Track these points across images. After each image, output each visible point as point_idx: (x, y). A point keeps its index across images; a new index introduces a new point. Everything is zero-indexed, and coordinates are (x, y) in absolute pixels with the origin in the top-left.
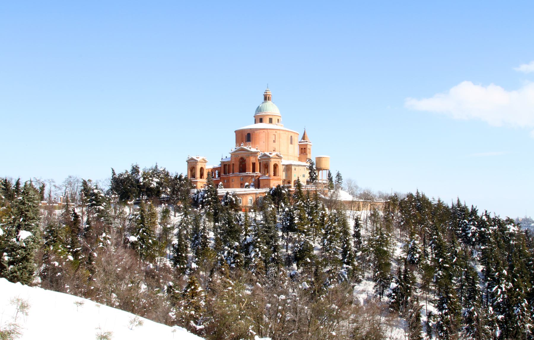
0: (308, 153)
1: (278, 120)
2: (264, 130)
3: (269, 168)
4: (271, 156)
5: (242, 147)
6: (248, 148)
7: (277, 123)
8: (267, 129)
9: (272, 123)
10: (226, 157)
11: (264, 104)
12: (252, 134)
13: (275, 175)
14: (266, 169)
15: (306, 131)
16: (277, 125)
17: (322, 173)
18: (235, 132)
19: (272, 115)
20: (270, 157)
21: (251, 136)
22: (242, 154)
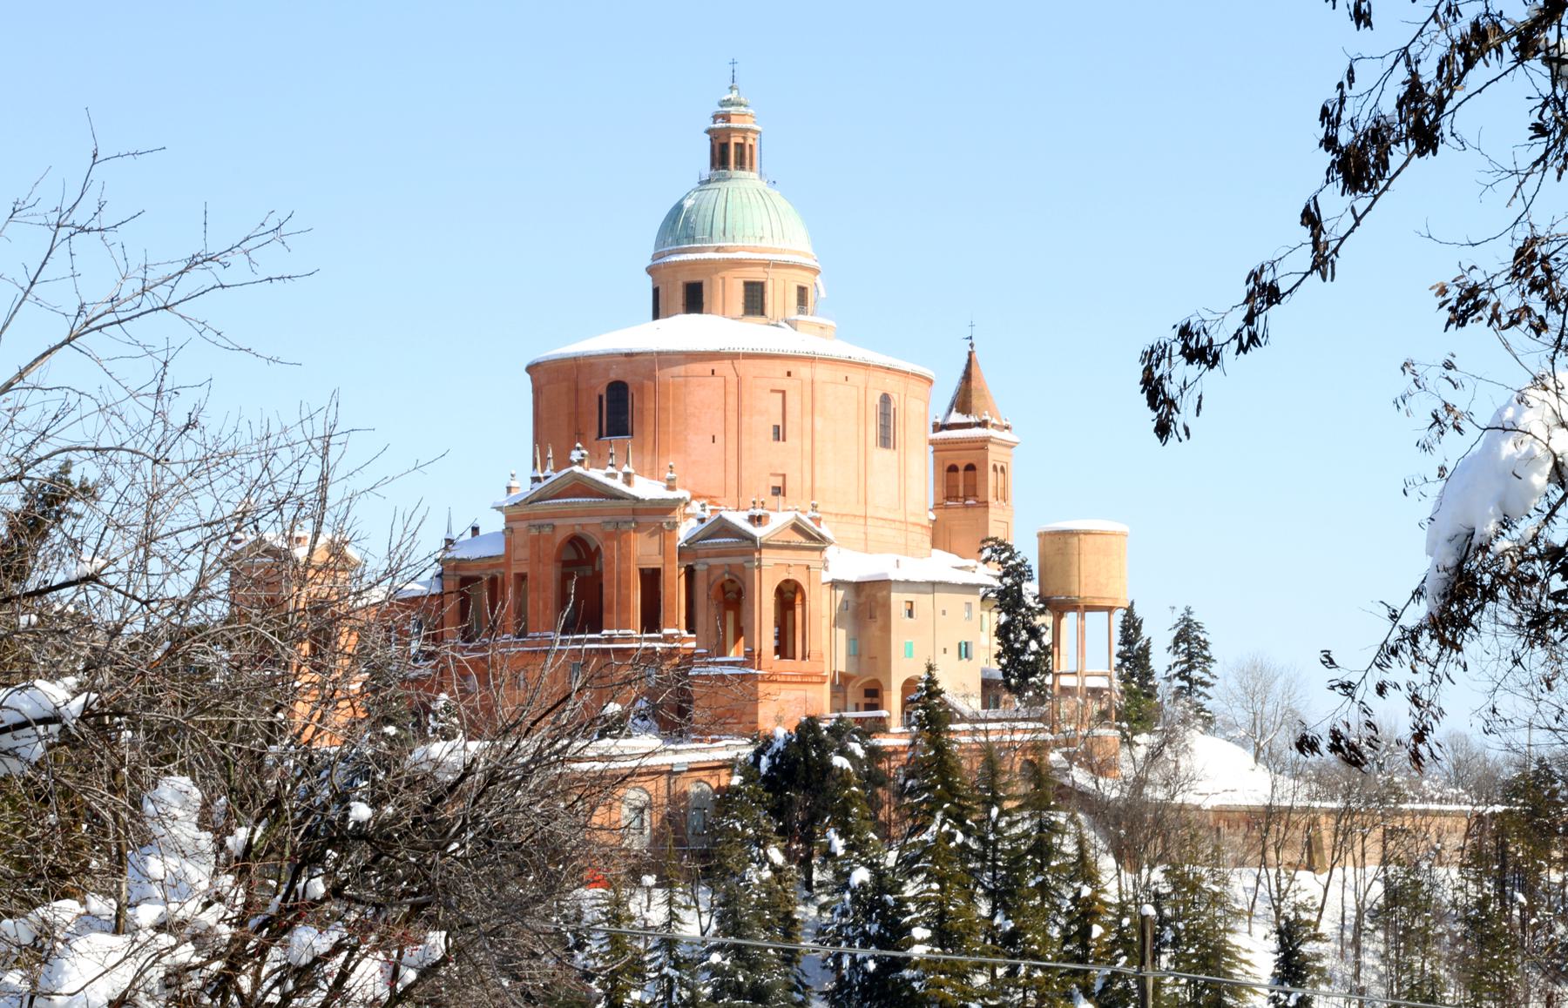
0: (991, 499)
1: (802, 291)
2: (715, 365)
3: (745, 606)
4: (759, 532)
5: (577, 469)
6: (613, 476)
7: (793, 314)
8: (734, 356)
9: (762, 313)
10: (475, 530)
11: (711, 194)
12: (641, 388)
13: (784, 648)
14: (730, 616)
15: (977, 355)
16: (793, 324)
17: (1081, 633)
18: (531, 369)
19: (766, 264)
20: (752, 539)
21: (635, 402)
22: (578, 517)
